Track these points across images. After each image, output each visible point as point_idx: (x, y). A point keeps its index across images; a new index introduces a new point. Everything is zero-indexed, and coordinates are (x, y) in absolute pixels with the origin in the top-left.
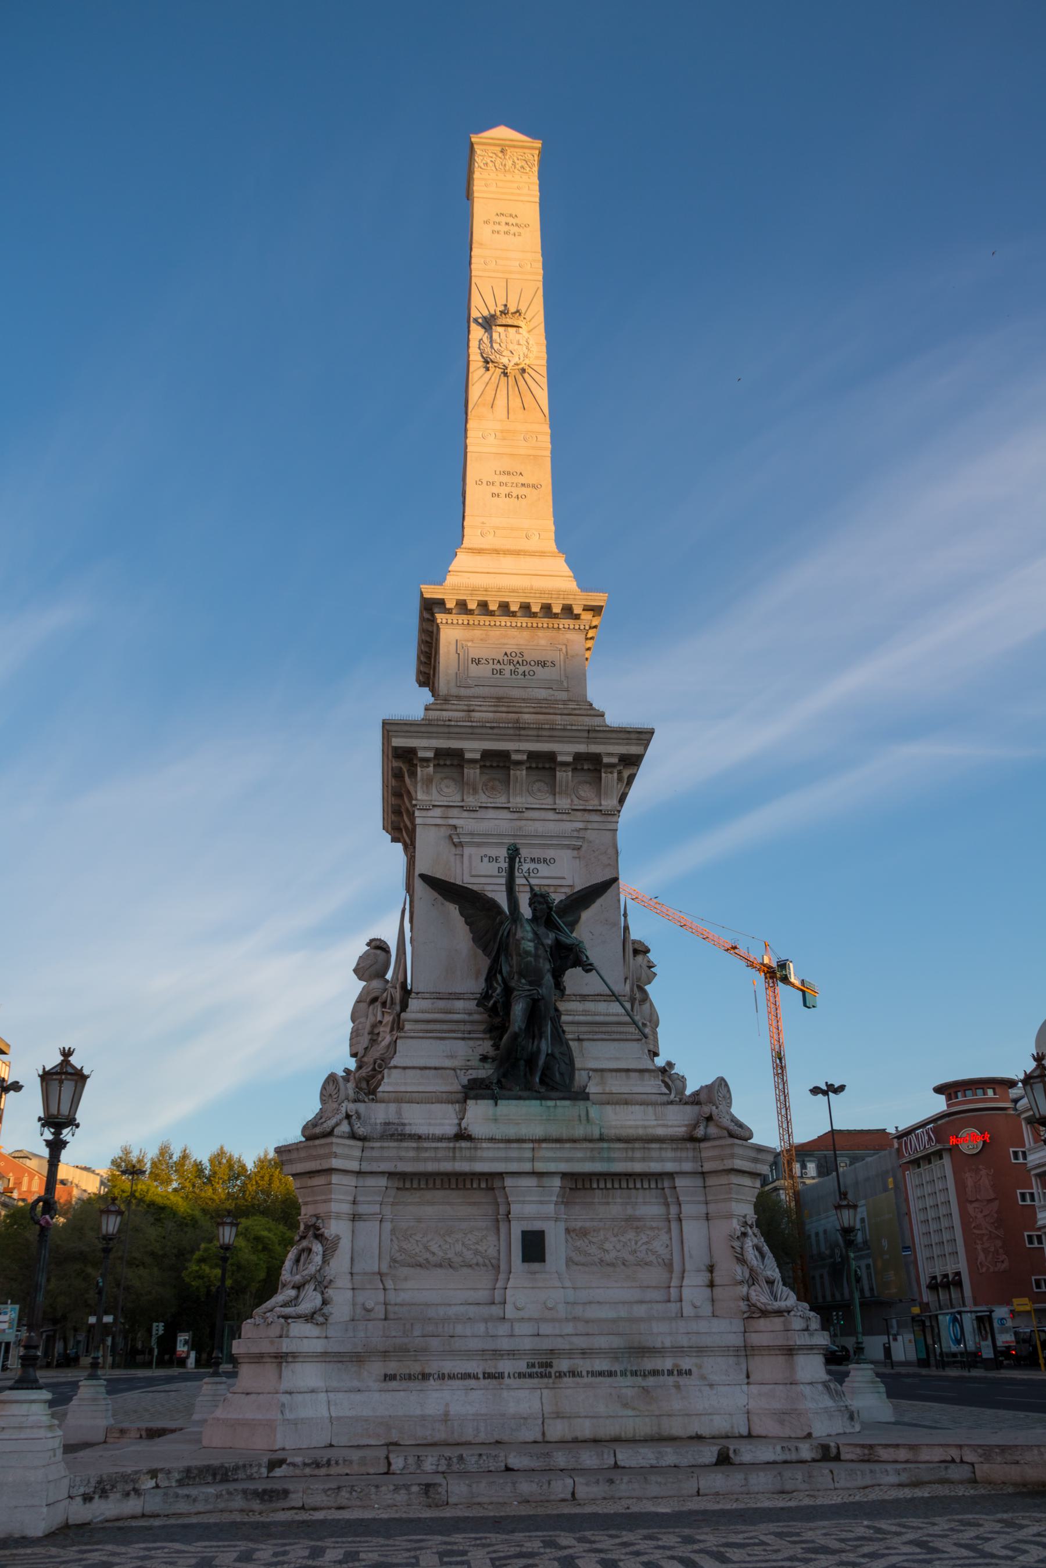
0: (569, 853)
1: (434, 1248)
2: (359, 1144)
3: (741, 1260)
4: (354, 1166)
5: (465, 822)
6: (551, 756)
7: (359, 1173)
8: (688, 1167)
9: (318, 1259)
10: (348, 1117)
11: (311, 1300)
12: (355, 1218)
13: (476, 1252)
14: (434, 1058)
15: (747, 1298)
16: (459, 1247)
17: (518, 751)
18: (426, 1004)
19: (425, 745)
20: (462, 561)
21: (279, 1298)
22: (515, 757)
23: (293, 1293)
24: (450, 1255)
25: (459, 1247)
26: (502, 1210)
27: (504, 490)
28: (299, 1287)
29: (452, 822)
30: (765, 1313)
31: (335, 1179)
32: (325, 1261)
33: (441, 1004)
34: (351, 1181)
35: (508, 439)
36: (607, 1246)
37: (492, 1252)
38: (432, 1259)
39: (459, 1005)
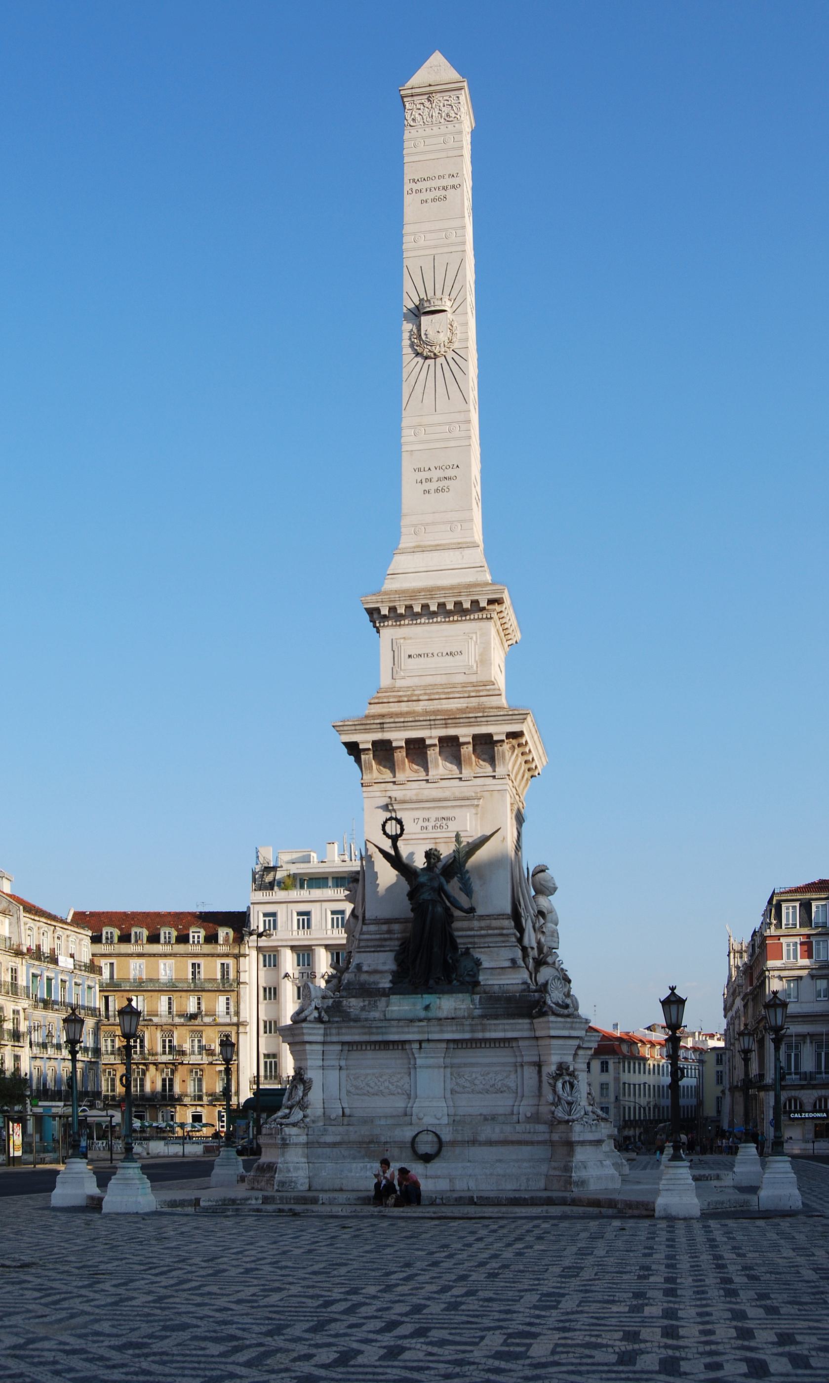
0: (473, 811)
1: (372, 1085)
2: (322, 1026)
3: (554, 1091)
4: (320, 1038)
5: (397, 793)
6: (455, 738)
7: (324, 1043)
8: (526, 1034)
9: (300, 1093)
10: (316, 1008)
11: (297, 1115)
12: (323, 1068)
13: (397, 1087)
14: (381, 964)
15: (553, 1113)
16: (387, 1084)
17: (430, 737)
18: (372, 928)
19: (365, 740)
20: (400, 562)
21: (280, 1114)
22: (428, 742)
23: (287, 1111)
24: (382, 1088)
25: (387, 1084)
26: (412, 1062)
27: (433, 486)
28: (291, 1108)
29: (389, 794)
30: (560, 1122)
31: (308, 1047)
32: (305, 1094)
33: (384, 927)
34: (319, 1047)
35: (444, 421)
36: (477, 1082)
37: (407, 1087)
38: (371, 1090)
39: (396, 927)
